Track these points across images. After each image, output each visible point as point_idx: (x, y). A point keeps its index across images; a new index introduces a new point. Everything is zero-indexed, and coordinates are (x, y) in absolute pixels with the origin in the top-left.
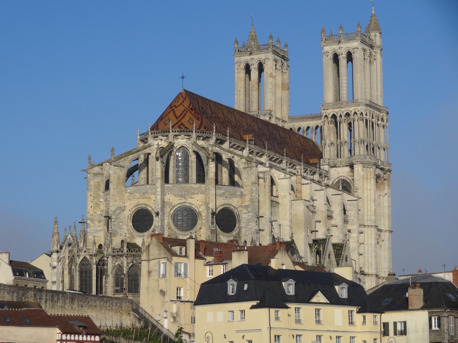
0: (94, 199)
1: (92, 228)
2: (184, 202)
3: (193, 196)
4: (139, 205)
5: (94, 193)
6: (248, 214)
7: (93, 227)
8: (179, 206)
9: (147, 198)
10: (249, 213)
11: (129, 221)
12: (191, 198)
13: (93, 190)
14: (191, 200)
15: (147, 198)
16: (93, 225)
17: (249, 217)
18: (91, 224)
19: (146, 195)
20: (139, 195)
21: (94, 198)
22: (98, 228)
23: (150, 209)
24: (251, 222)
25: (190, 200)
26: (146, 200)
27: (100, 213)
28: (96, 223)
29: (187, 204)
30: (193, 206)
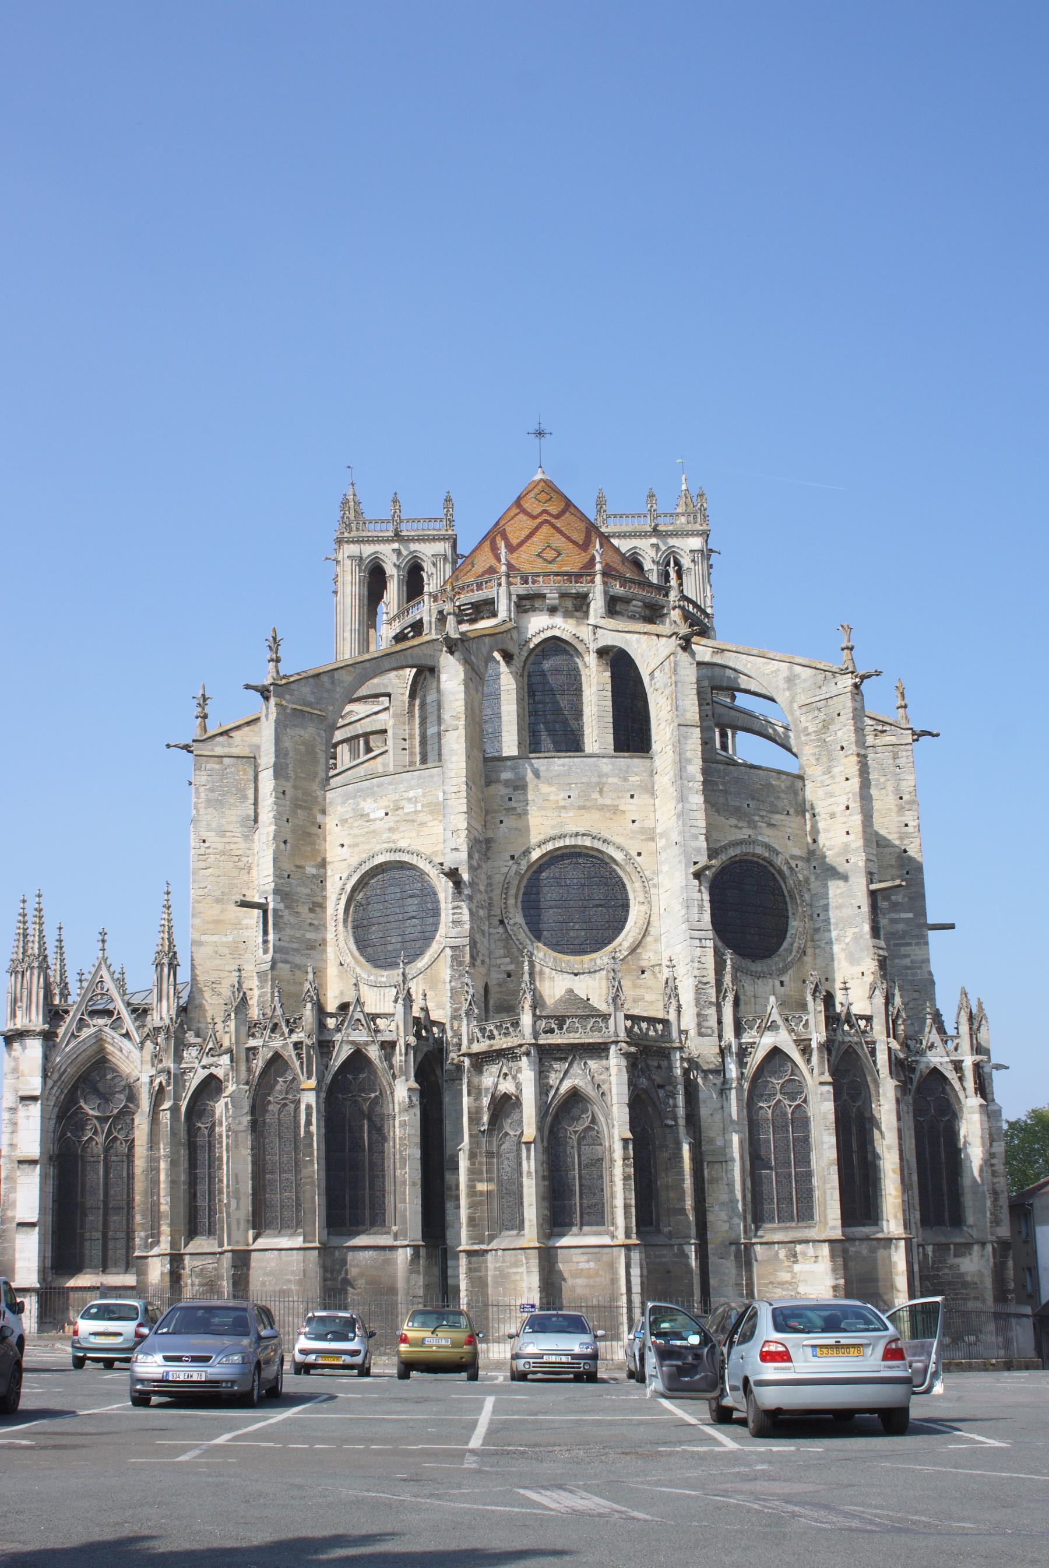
0: (294, 813)
1: (289, 931)
2: (750, 842)
3: (777, 818)
4: (562, 836)
5: (295, 787)
6: (894, 916)
7: (292, 926)
8: (732, 852)
9: (602, 808)
10: (897, 911)
11: (511, 901)
12: (770, 825)
13: (292, 774)
14: (767, 831)
15: (602, 808)
16: (293, 920)
17: (900, 927)
18: (286, 913)
19: (596, 795)
20: (564, 795)
21: (297, 805)
22: (309, 935)
23: (619, 856)
24: (909, 944)
25: (766, 835)
26: (596, 815)
27: (314, 871)
28: (304, 910)
29: (759, 850)
30: (779, 861)
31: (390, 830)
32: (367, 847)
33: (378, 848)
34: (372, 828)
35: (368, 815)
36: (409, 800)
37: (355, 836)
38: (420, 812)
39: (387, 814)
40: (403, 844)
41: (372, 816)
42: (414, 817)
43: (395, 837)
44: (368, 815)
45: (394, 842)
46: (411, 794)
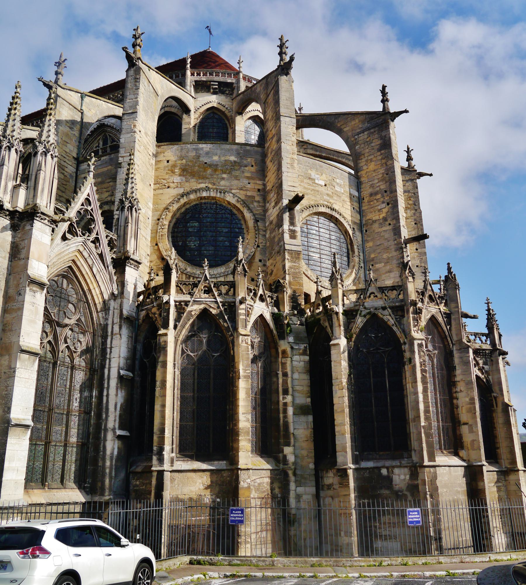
31: (328, 195)
32: (313, 198)
33: (321, 202)
34: (317, 188)
35: (314, 180)
36: (338, 184)
37: (305, 188)
38: (343, 194)
39: (325, 185)
40: (335, 206)
41: (317, 181)
42: (341, 195)
43: (331, 201)
44: (314, 180)
45: (330, 203)
46: (338, 181)
